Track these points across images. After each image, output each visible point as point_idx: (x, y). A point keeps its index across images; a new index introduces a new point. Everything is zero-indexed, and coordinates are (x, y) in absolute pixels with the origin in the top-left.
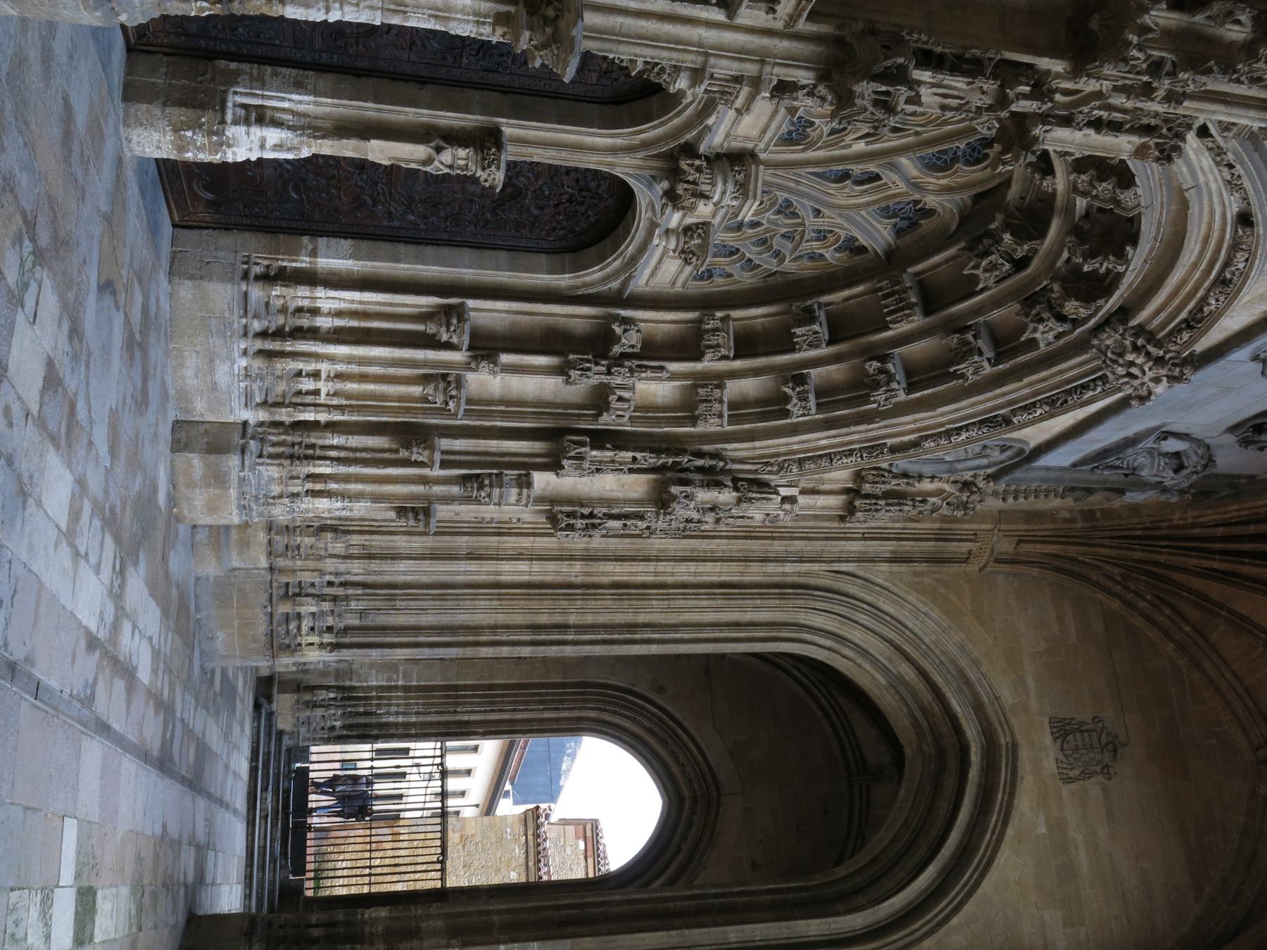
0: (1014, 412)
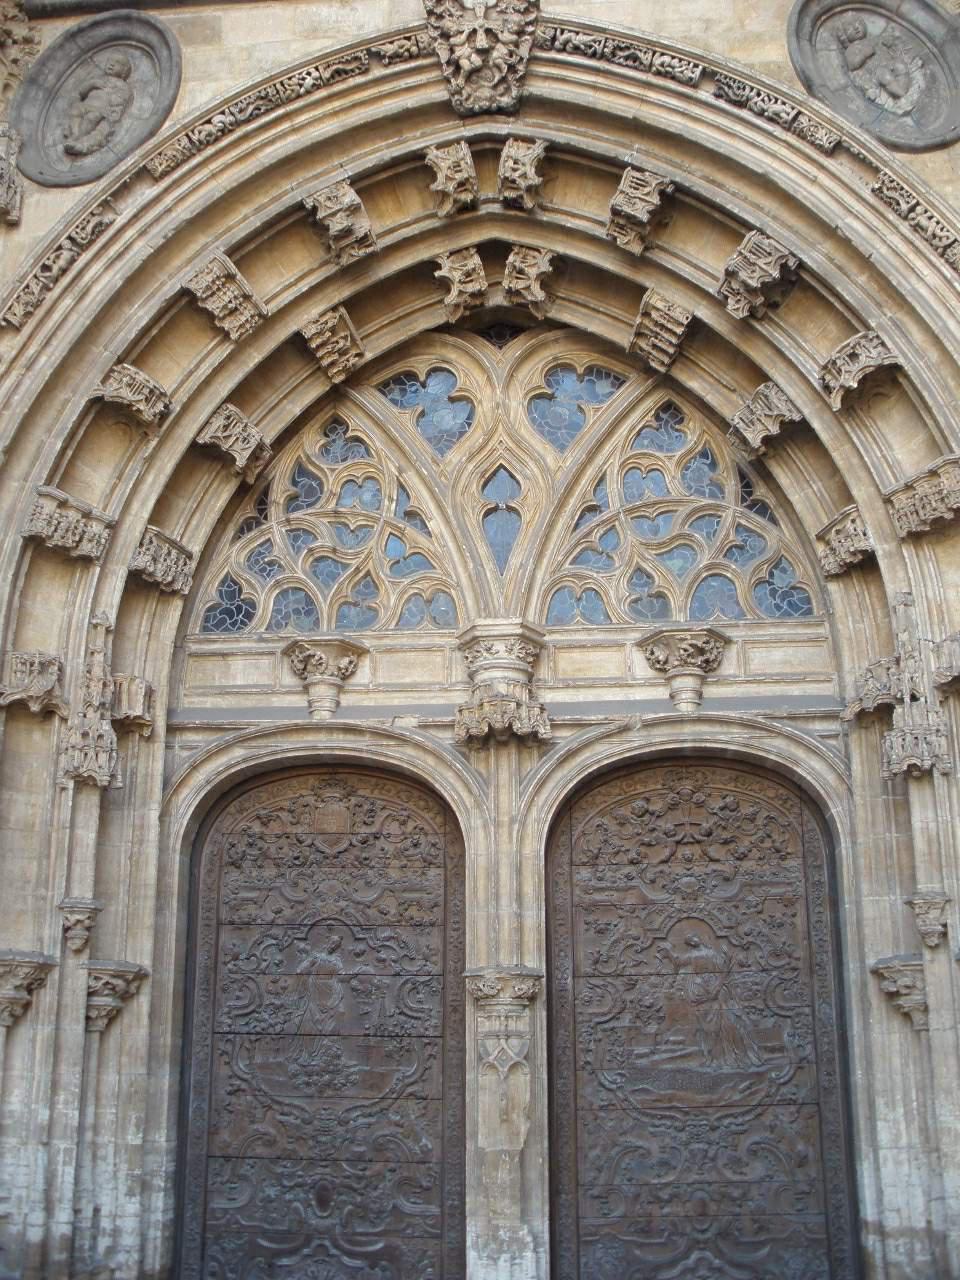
0: (690, 83)
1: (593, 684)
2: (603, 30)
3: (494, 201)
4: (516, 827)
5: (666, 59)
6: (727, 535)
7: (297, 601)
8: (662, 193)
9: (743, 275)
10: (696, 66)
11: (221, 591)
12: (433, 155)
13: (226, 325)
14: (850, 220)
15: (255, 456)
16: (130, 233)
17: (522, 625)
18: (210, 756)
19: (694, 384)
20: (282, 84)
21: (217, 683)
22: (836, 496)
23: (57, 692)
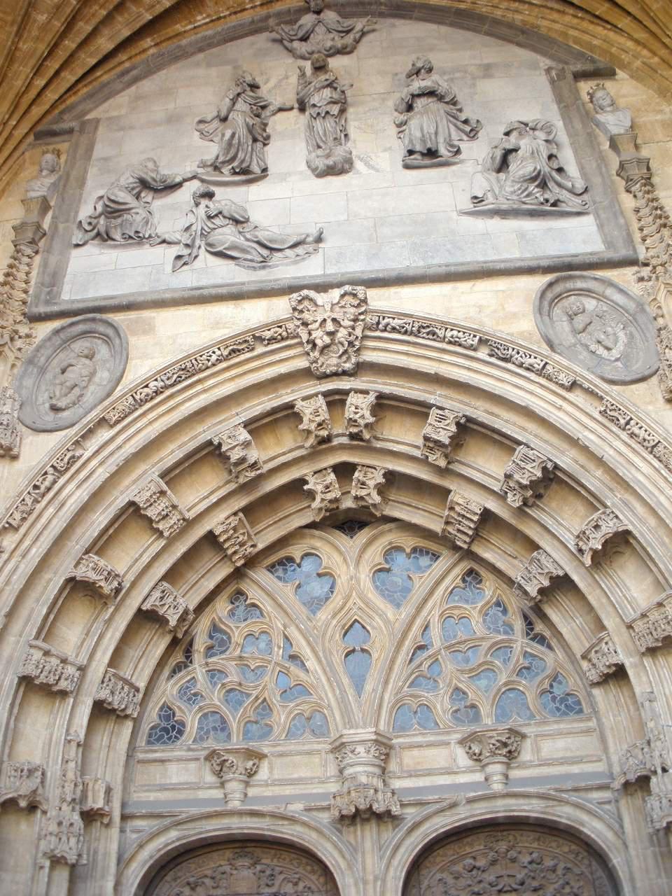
0: (471, 348)
1: (429, 773)
2: (411, 316)
3: (343, 435)
4: (379, 883)
5: (455, 333)
6: (518, 661)
7: (215, 721)
8: (458, 424)
9: (517, 477)
10: (475, 336)
11: (160, 716)
12: (299, 405)
13: (161, 526)
14: (587, 433)
15: (182, 619)
16: (94, 463)
17: (376, 733)
18: (153, 836)
19: (487, 555)
20: (196, 360)
21: (158, 782)
22: (592, 626)
23: (40, 791)
